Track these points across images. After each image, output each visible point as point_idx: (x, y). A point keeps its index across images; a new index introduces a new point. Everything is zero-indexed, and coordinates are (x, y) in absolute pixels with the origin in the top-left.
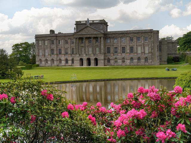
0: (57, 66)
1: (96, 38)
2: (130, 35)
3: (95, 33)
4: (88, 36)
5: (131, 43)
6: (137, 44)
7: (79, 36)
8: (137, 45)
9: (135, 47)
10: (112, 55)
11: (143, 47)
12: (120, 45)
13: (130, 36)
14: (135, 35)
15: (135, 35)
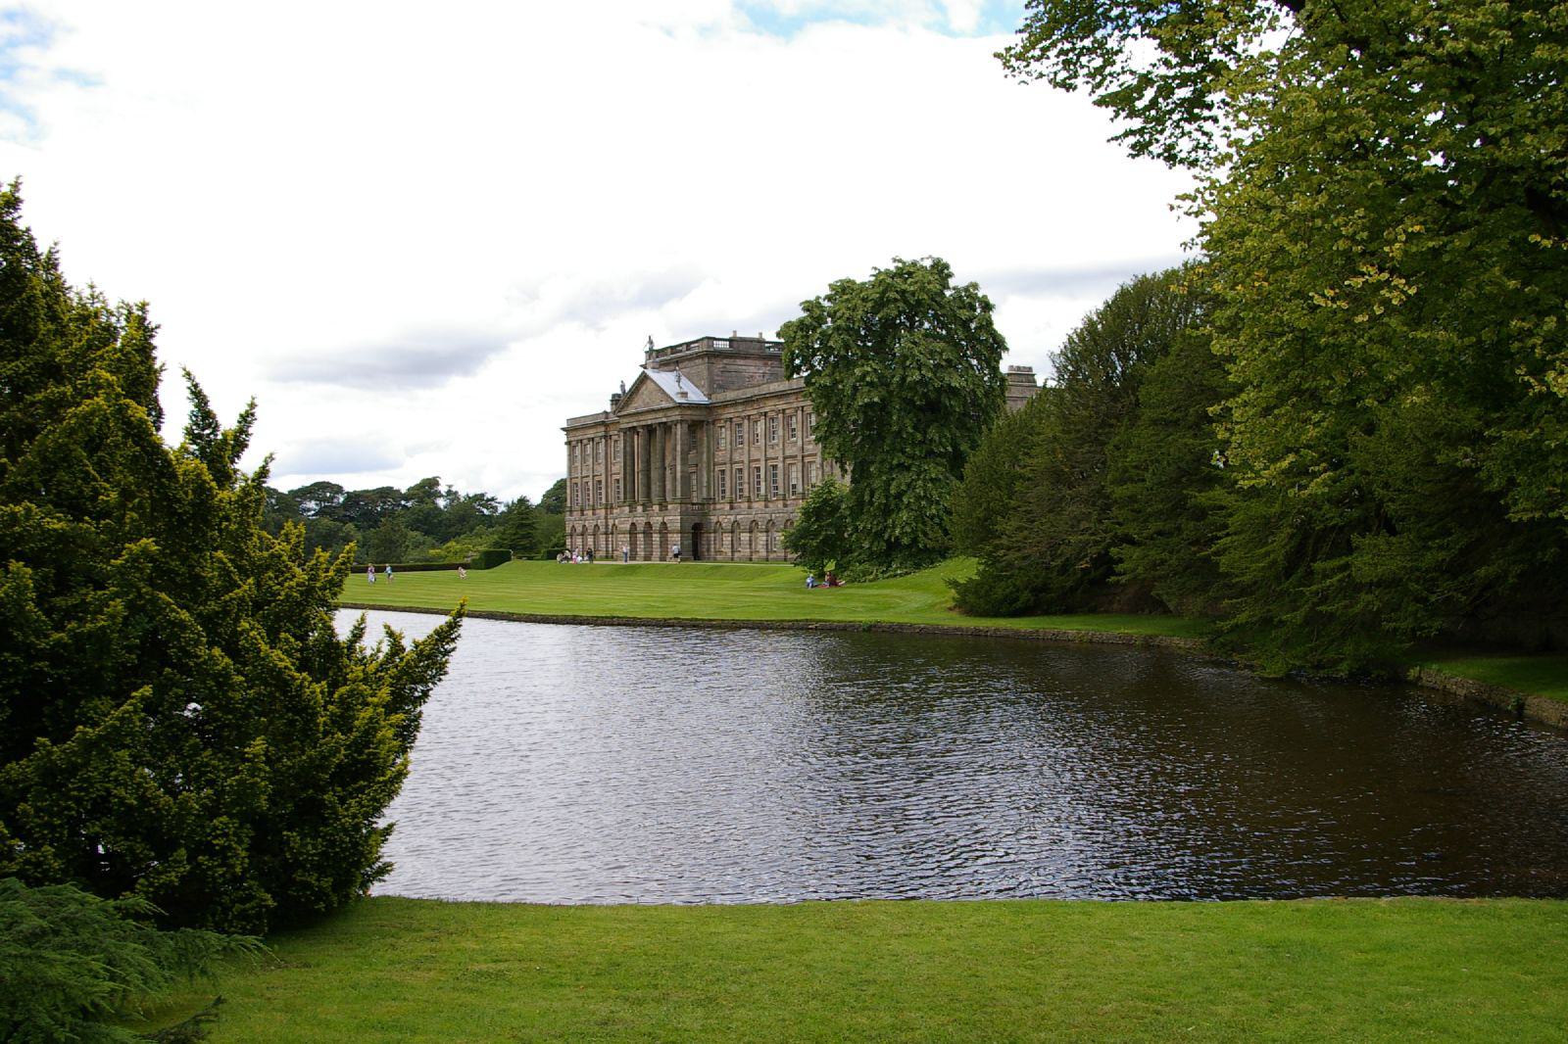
0: (607, 558)
1: (667, 428)
2: (769, 406)
3: (664, 405)
4: (649, 420)
5: (773, 447)
6: (788, 453)
7: (631, 419)
8: (785, 458)
9: (780, 465)
10: (727, 507)
11: (800, 465)
12: (746, 462)
13: (767, 409)
14: (781, 405)
15: (780, 407)
